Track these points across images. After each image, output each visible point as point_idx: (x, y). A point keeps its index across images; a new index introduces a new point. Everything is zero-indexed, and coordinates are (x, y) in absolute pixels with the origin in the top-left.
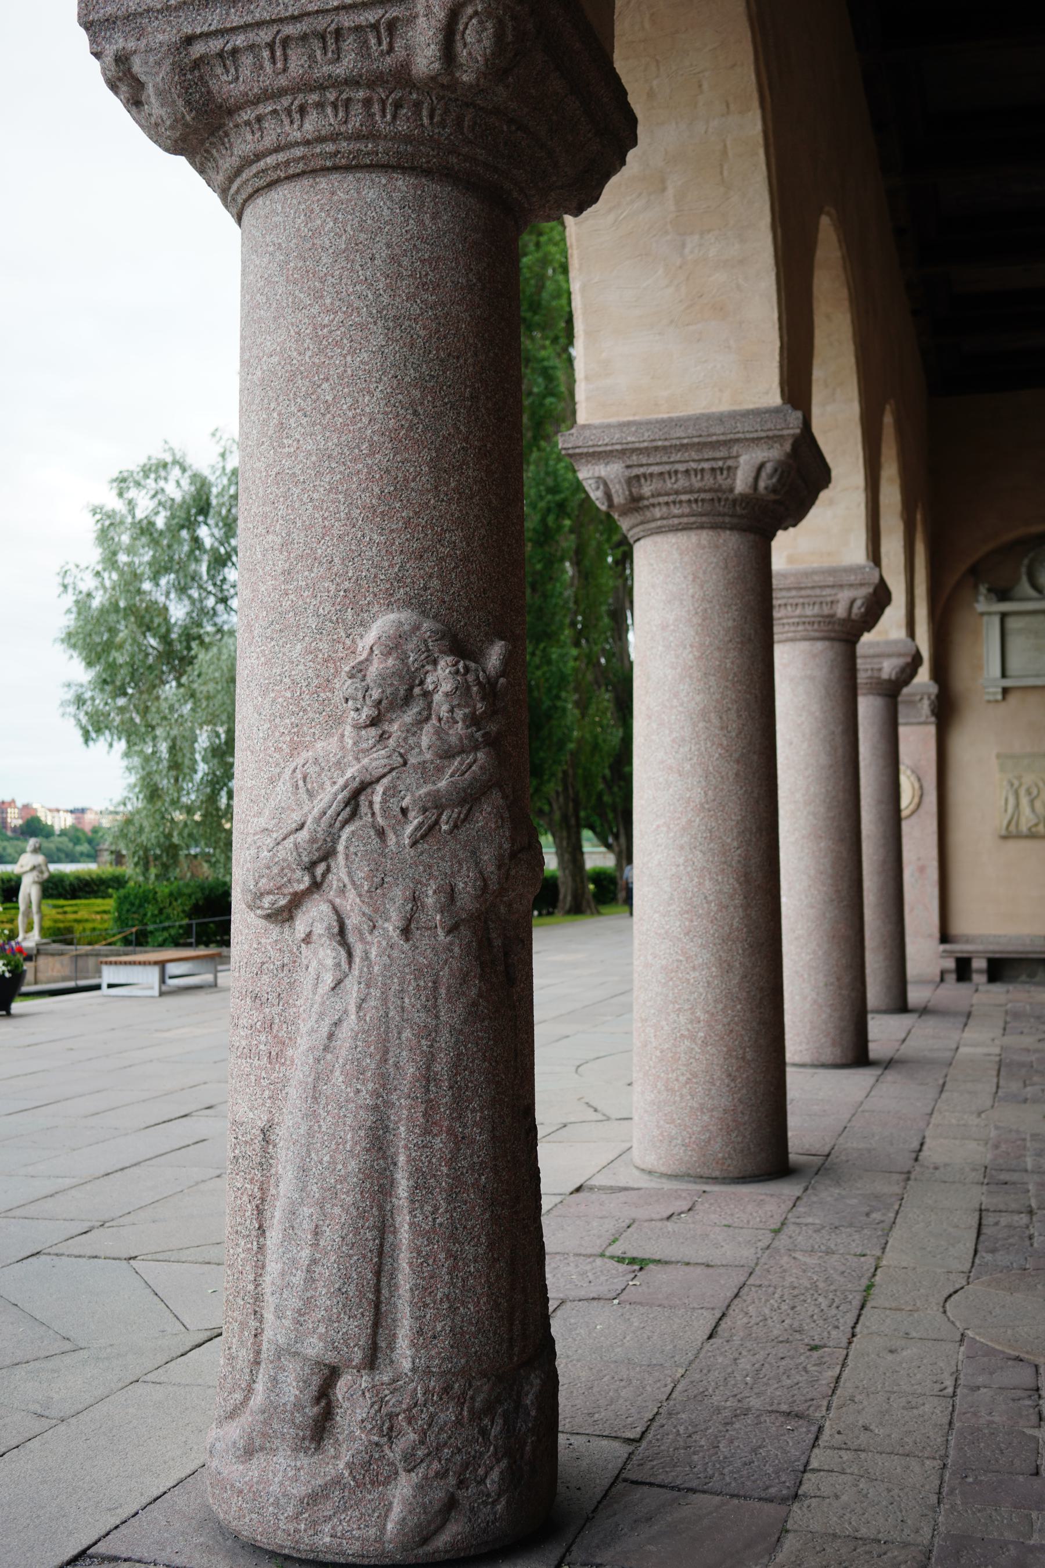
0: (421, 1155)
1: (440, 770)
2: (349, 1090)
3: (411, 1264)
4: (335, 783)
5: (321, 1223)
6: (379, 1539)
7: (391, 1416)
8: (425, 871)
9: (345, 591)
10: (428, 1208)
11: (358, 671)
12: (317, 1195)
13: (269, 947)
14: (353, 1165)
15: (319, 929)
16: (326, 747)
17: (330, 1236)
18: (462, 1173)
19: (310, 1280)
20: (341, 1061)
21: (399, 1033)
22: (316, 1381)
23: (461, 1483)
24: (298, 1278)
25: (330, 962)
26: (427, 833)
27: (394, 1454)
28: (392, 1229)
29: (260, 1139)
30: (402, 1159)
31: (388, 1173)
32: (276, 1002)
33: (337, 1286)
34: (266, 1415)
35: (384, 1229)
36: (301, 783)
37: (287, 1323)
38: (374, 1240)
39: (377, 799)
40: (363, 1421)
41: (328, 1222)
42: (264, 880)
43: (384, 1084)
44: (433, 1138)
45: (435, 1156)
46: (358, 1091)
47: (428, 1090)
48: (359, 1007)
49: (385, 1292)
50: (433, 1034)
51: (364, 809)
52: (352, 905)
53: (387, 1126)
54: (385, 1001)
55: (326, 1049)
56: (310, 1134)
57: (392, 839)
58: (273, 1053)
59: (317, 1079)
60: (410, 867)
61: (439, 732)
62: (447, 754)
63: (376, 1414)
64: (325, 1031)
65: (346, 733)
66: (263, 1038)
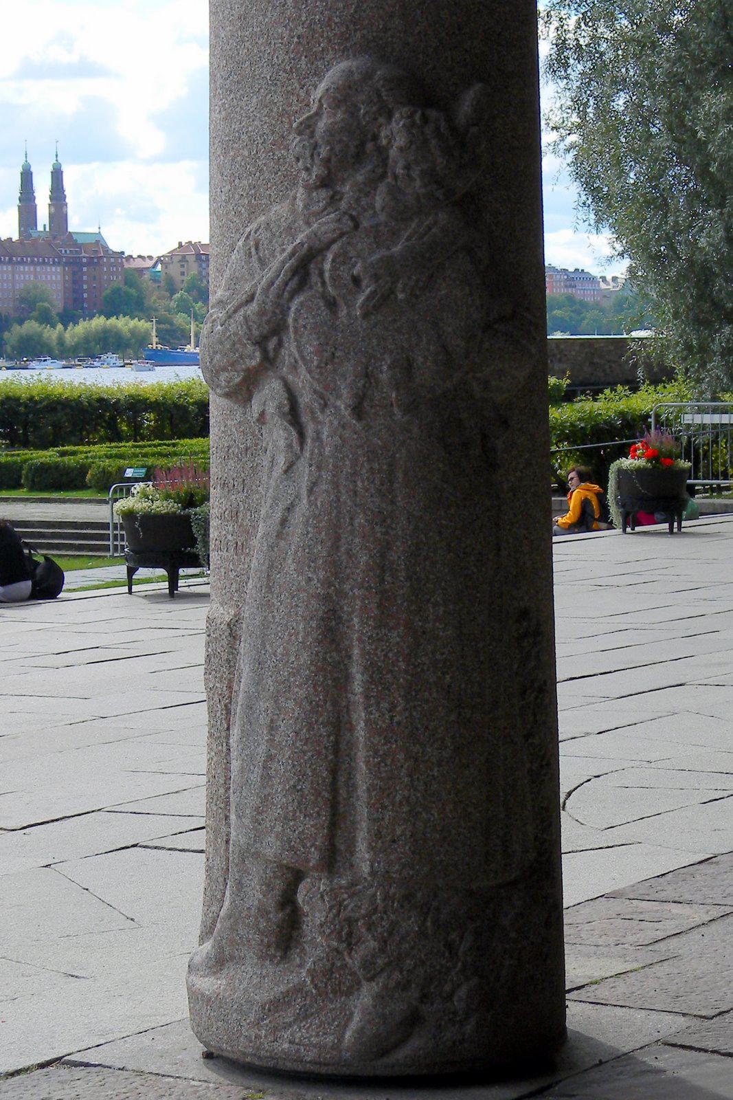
0: (376, 649)
1: (395, 234)
2: (300, 578)
3: (367, 763)
4: (284, 250)
5: (276, 717)
6: (336, 1047)
7: (350, 922)
8: (378, 345)
9: (299, 37)
10: (385, 705)
11: (307, 127)
12: (272, 689)
13: (234, 430)
14: (305, 657)
15: (271, 409)
16: (280, 210)
17: (286, 729)
18: (422, 670)
19: (266, 777)
20: (293, 547)
21: (351, 519)
22: (279, 885)
23: (424, 997)
24: (255, 777)
25: (282, 443)
26: (381, 301)
27: (354, 961)
28: (347, 726)
29: (227, 634)
30: (356, 651)
31: (342, 667)
32: (240, 489)
33: (292, 783)
34: (232, 920)
35: (340, 725)
36: (253, 250)
37: (246, 821)
38: (329, 736)
39: (327, 266)
40: (321, 925)
41: (282, 716)
42: (218, 357)
43: (336, 571)
44: (389, 631)
45: (391, 650)
46: (310, 579)
47: (382, 581)
48: (311, 491)
49: (343, 792)
50: (389, 521)
51: (315, 278)
52: (303, 381)
53: (340, 618)
54: (336, 485)
55: (279, 535)
56: (265, 625)
57: (343, 312)
58: (239, 543)
59: (271, 567)
60: (363, 340)
61: (394, 192)
62: (401, 214)
63: (334, 919)
64: (278, 515)
65: (298, 195)
66: (231, 529)
